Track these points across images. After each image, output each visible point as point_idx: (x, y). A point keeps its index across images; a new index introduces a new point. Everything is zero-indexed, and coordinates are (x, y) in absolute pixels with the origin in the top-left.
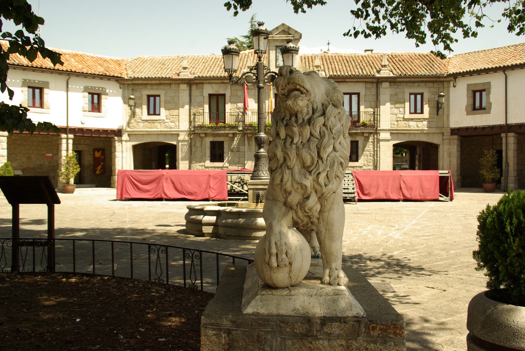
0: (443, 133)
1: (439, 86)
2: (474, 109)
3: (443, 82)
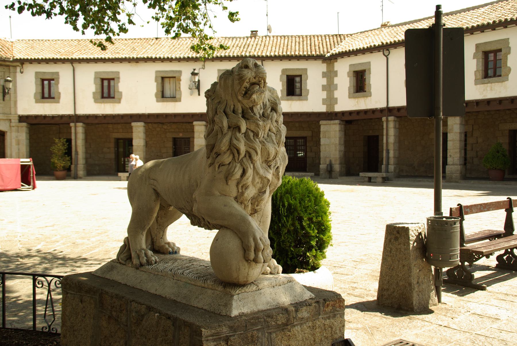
0: (10, 120)
1: (4, 70)
2: (43, 97)
3: (9, 66)
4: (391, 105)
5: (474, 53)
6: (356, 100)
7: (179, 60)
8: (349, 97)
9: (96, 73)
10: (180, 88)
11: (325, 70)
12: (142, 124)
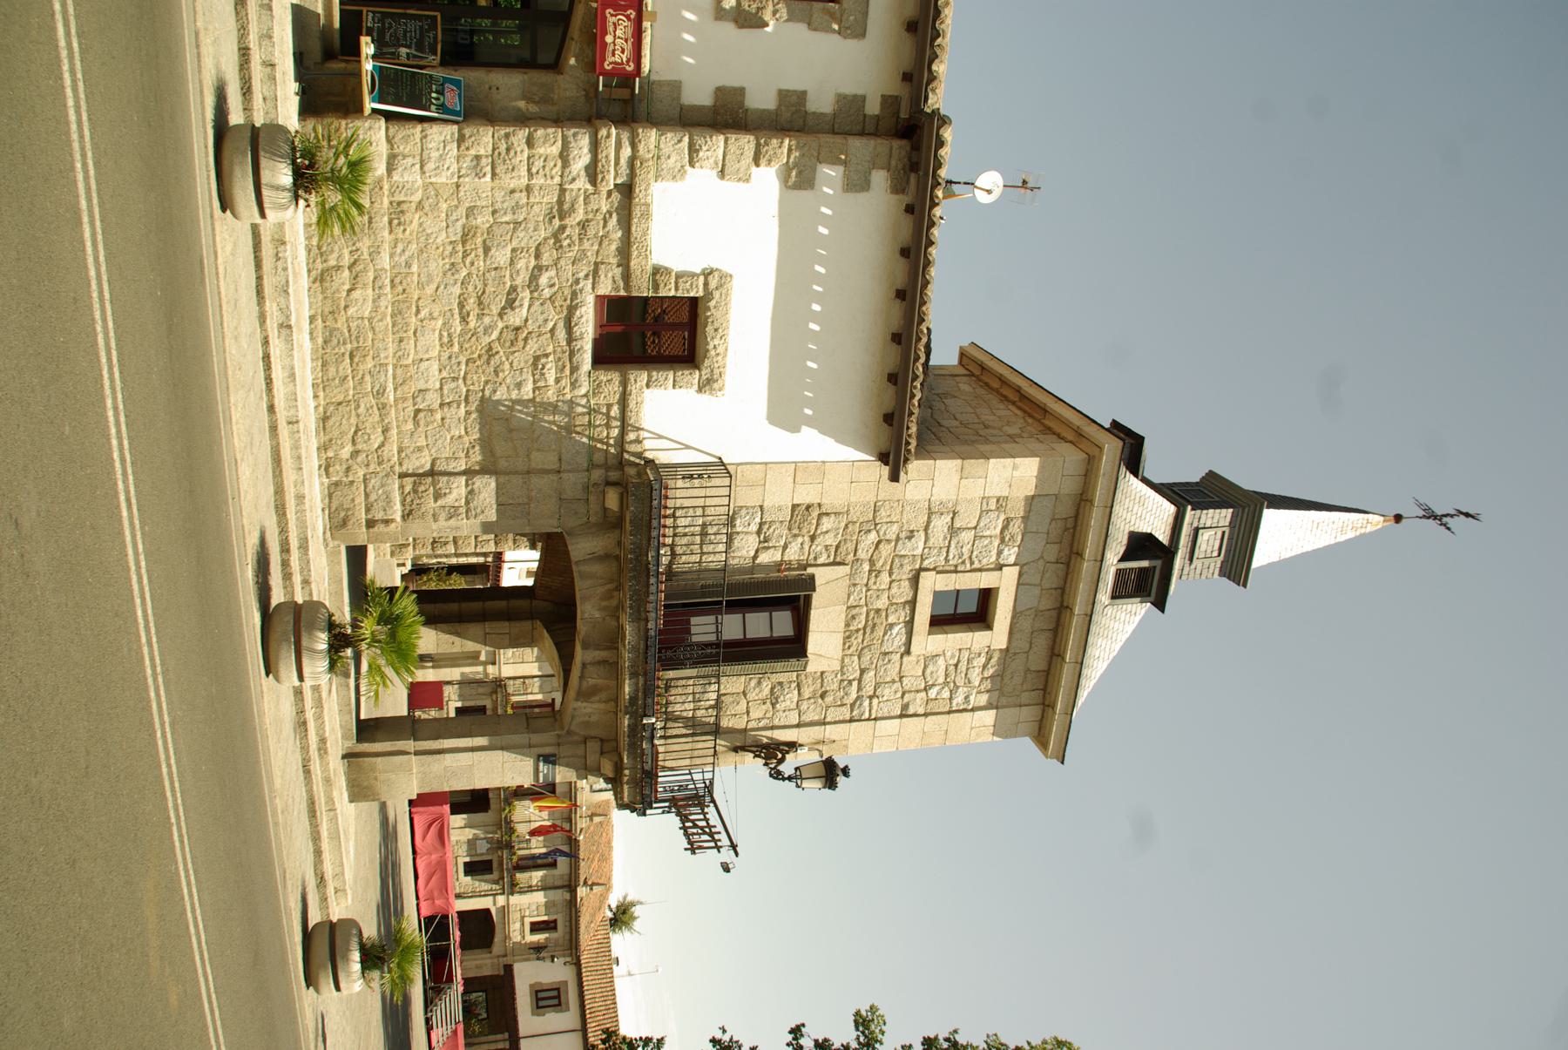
2: (537, 992)
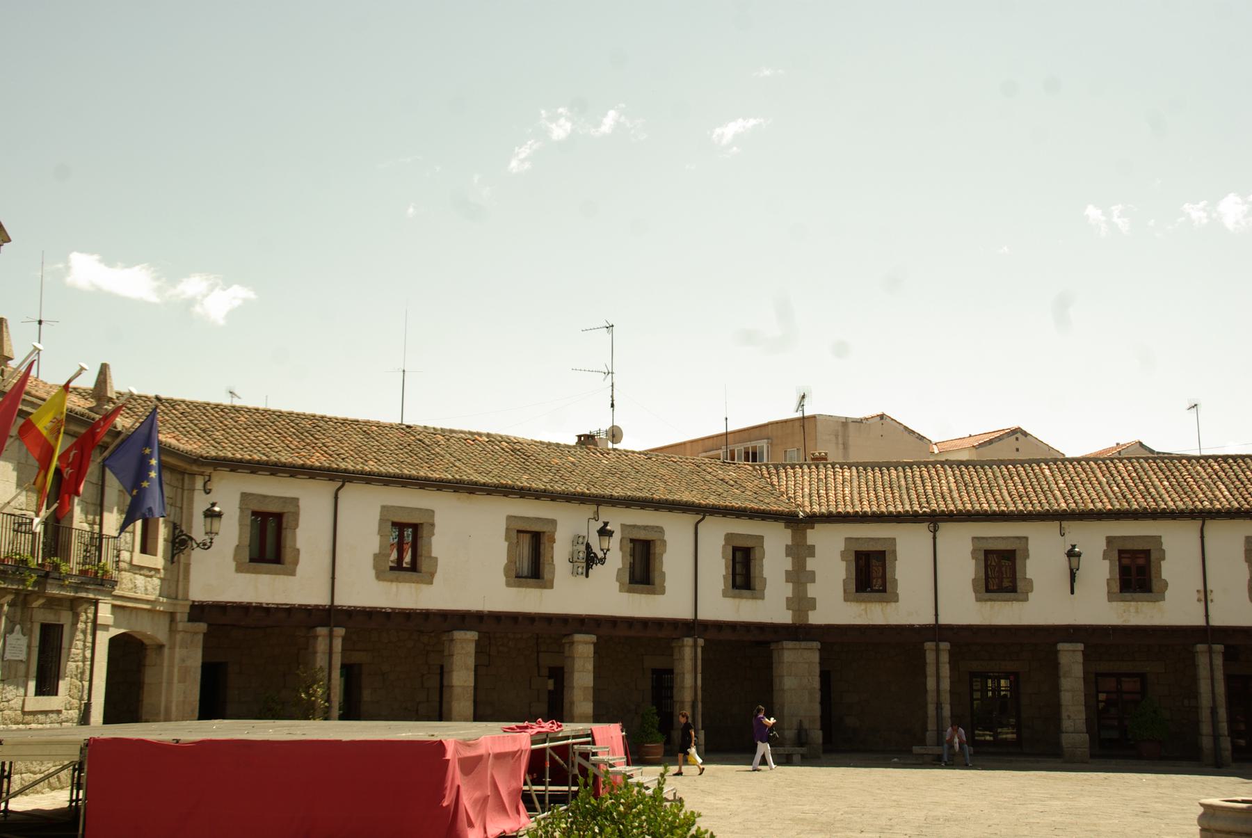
4: (943, 620)
5: (1105, 551)
6: (863, 606)
7: (553, 496)
8: (846, 600)
9: (384, 508)
10: (552, 558)
11: (790, 543)
12: (472, 635)
